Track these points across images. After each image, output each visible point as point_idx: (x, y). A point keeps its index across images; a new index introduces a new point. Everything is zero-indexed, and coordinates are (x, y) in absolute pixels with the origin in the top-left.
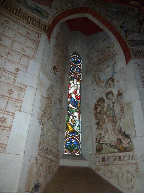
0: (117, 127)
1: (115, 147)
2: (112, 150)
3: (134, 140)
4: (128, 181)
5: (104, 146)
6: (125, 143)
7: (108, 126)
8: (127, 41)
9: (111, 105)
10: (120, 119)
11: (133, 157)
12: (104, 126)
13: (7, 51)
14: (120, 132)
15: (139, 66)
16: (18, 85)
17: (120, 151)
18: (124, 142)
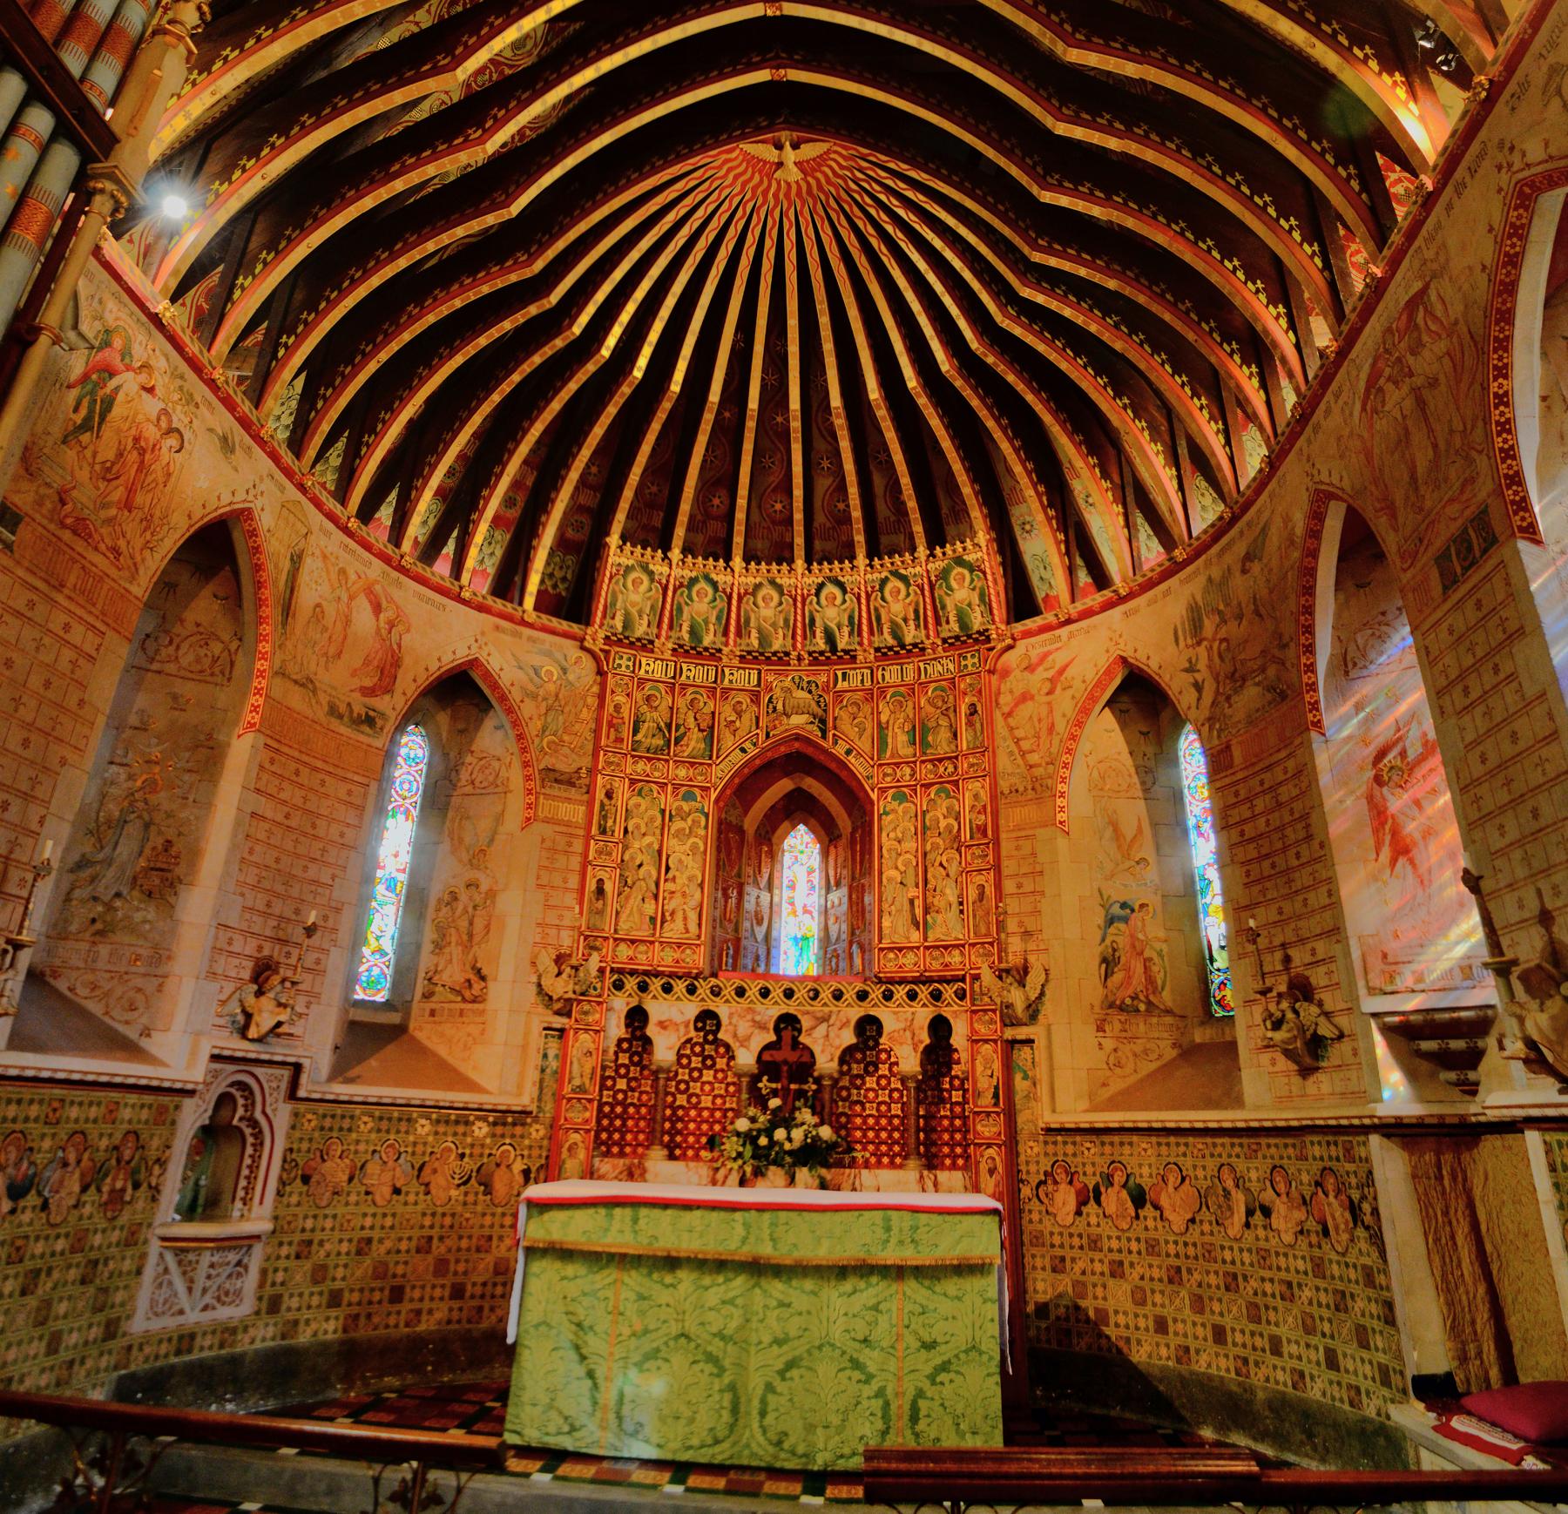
0: (471, 956)
1: (459, 993)
2: (452, 997)
3: (491, 984)
4: (466, 1048)
5: (439, 989)
6: (477, 986)
7: (455, 951)
8: (540, 771)
9: (470, 910)
10: (479, 944)
11: (483, 1012)
12: (447, 950)
13: (321, 845)
14: (473, 968)
15: (543, 840)
16: (333, 904)
17: (464, 1000)
18: (475, 986)
